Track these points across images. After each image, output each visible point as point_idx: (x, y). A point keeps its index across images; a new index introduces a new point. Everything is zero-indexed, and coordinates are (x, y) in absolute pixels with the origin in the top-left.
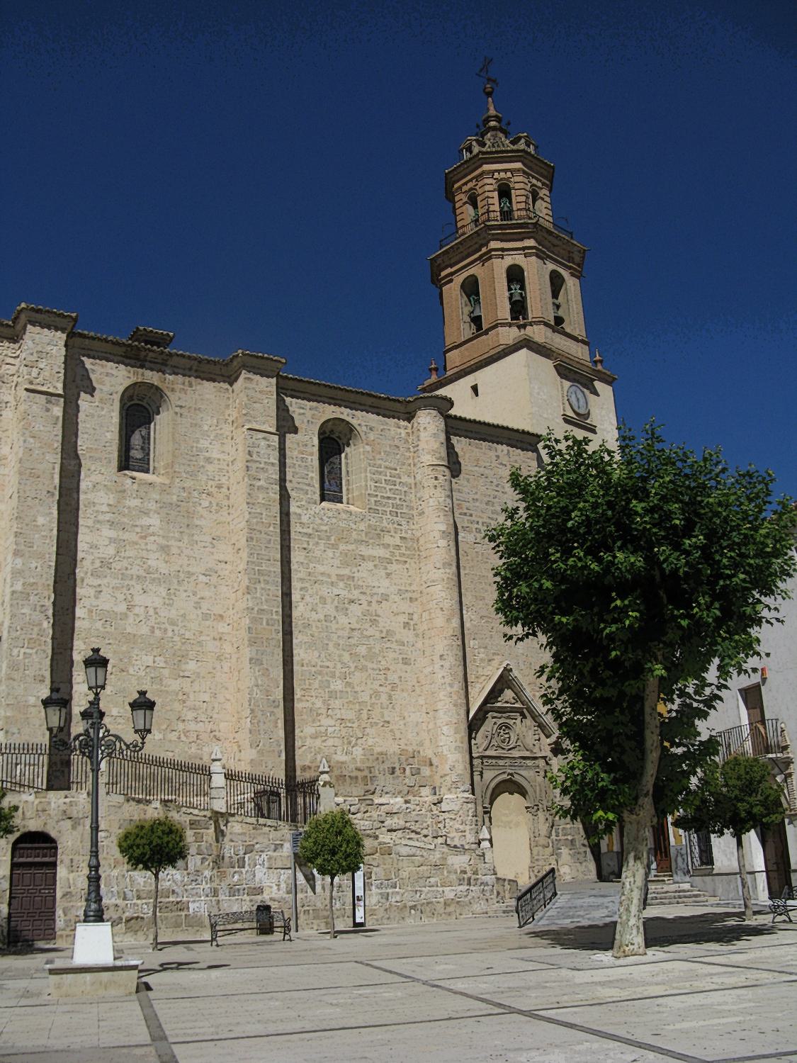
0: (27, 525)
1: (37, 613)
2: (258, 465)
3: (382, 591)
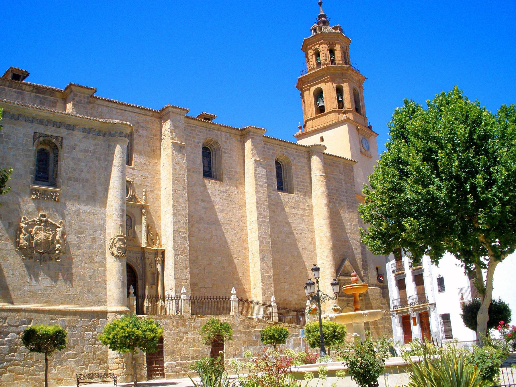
1: (183, 240)
3: (301, 228)
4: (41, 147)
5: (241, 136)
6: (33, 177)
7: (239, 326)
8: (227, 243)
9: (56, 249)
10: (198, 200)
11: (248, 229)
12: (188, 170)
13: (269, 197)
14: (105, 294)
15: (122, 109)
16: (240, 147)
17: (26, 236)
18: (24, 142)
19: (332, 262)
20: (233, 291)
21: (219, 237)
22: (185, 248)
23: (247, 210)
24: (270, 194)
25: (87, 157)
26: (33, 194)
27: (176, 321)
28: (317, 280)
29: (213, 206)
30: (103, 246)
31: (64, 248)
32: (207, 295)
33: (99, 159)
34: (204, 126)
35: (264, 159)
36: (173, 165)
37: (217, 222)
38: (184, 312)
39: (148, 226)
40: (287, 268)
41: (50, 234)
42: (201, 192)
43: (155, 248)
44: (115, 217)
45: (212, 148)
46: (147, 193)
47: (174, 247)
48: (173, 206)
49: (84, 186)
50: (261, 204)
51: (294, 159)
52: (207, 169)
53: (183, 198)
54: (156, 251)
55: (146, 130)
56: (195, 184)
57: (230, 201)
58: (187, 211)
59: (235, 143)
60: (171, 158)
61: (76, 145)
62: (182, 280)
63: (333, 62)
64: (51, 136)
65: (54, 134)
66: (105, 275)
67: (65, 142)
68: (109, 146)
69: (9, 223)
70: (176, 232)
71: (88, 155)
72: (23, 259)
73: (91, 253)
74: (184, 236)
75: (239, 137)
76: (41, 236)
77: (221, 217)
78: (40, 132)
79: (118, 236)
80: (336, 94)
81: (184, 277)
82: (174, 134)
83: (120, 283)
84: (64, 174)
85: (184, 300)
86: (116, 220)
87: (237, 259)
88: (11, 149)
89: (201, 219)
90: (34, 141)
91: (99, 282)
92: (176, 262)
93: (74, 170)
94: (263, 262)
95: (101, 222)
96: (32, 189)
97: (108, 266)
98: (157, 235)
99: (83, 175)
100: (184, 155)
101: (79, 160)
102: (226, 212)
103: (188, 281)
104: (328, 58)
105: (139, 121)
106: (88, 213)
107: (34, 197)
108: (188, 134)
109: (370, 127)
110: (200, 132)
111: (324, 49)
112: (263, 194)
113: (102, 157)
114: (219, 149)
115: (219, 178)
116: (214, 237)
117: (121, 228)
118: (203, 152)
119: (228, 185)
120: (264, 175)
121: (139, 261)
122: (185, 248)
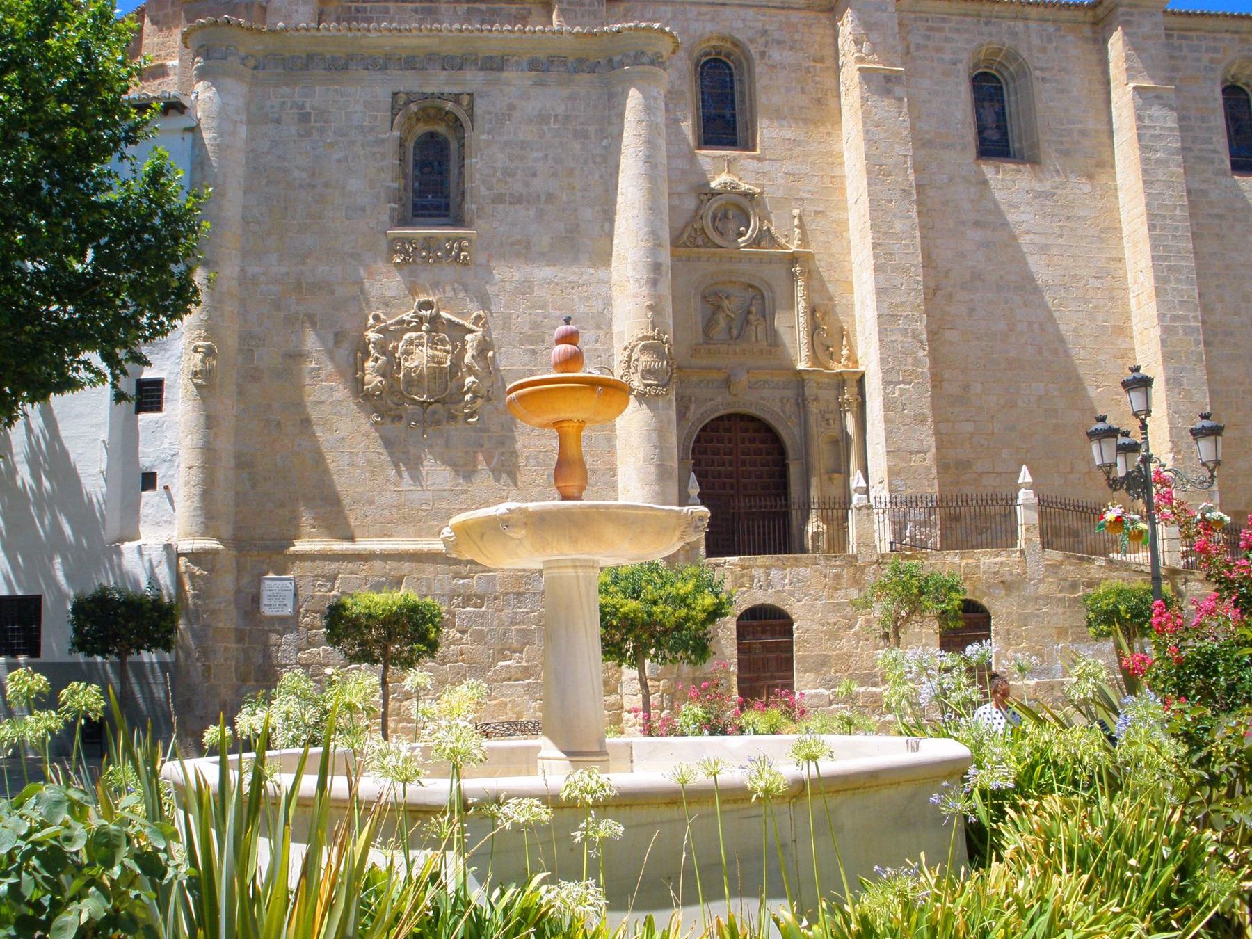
0: (885, 233)
1: (909, 340)
2: (1152, 132)
4: (422, 129)
5: (1095, 24)
6: (394, 209)
7: (1041, 581)
8: (1062, 341)
9: (466, 388)
10: (963, 223)
11: (1132, 295)
17: (379, 362)
18: (365, 124)
20: (1025, 476)
21: (1036, 326)
22: (917, 363)
23: (1125, 240)
25: (548, 136)
26: (396, 252)
27: (831, 572)
28: (1143, 422)
29: (1014, 238)
31: (489, 384)
33: (582, 135)
34: (970, 12)
35: (1170, 80)
36: (867, 132)
37: (1027, 285)
38: (858, 544)
39: (812, 311)
41: (445, 351)
43: (837, 368)
44: (632, 288)
45: (1006, 74)
46: (806, 219)
47: (883, 361)
48: (875, 246)
49: (541, 214)
50: (1164, 217)
52: (993, 135)
53: (906, 222)
54: (840, 378)
55: (791, 49)
56: (951, 180)
57: (1068, 218)
58: (920, 258)
59: (1075, 49)
60: (860, 113)
61: (512, 107)
62: (911, 453)
64: (441, 96)
65: (446, 90)
66: (612, 450)
67: (480, 106)
68: (611, 96)
69: (336, 334)
70: (886, 320)
71: (550, 129)
72: (376, 422)
74: (914, 330)
75: (1087, 31)
76: (420, 358)
77: (1036, 263)
78: (407, 89)
81: (915, 446)
82: (866, 47)
83: (653, 469)
84: (482, 188)
85: (859, 509)
86: (635, 296)
87: (1098, 387)
88: (332, 145)
89: (977, 276)
90: (394, 115)
92: (888, 405)
93: (509, 173)
94: (1177, 391)
95: (596, 306)
96: (395, 239)
98: (842, 333)
99: (538, 184)
100: (901, 100)
101: (524, 145)
102: (1054, 251)
103: (930, 455)
106: (557, 284)
107: (398, 261)
108: (921, 41)
110: (958, 31)
112: (1169, 185)
113: (592, 129)
114: (1023, 72)
115: (1029, 157)
117: (650, 314)
119: (1057, 171)
120: (1171, 129)
121: (791, 408)
122: (917, 363)
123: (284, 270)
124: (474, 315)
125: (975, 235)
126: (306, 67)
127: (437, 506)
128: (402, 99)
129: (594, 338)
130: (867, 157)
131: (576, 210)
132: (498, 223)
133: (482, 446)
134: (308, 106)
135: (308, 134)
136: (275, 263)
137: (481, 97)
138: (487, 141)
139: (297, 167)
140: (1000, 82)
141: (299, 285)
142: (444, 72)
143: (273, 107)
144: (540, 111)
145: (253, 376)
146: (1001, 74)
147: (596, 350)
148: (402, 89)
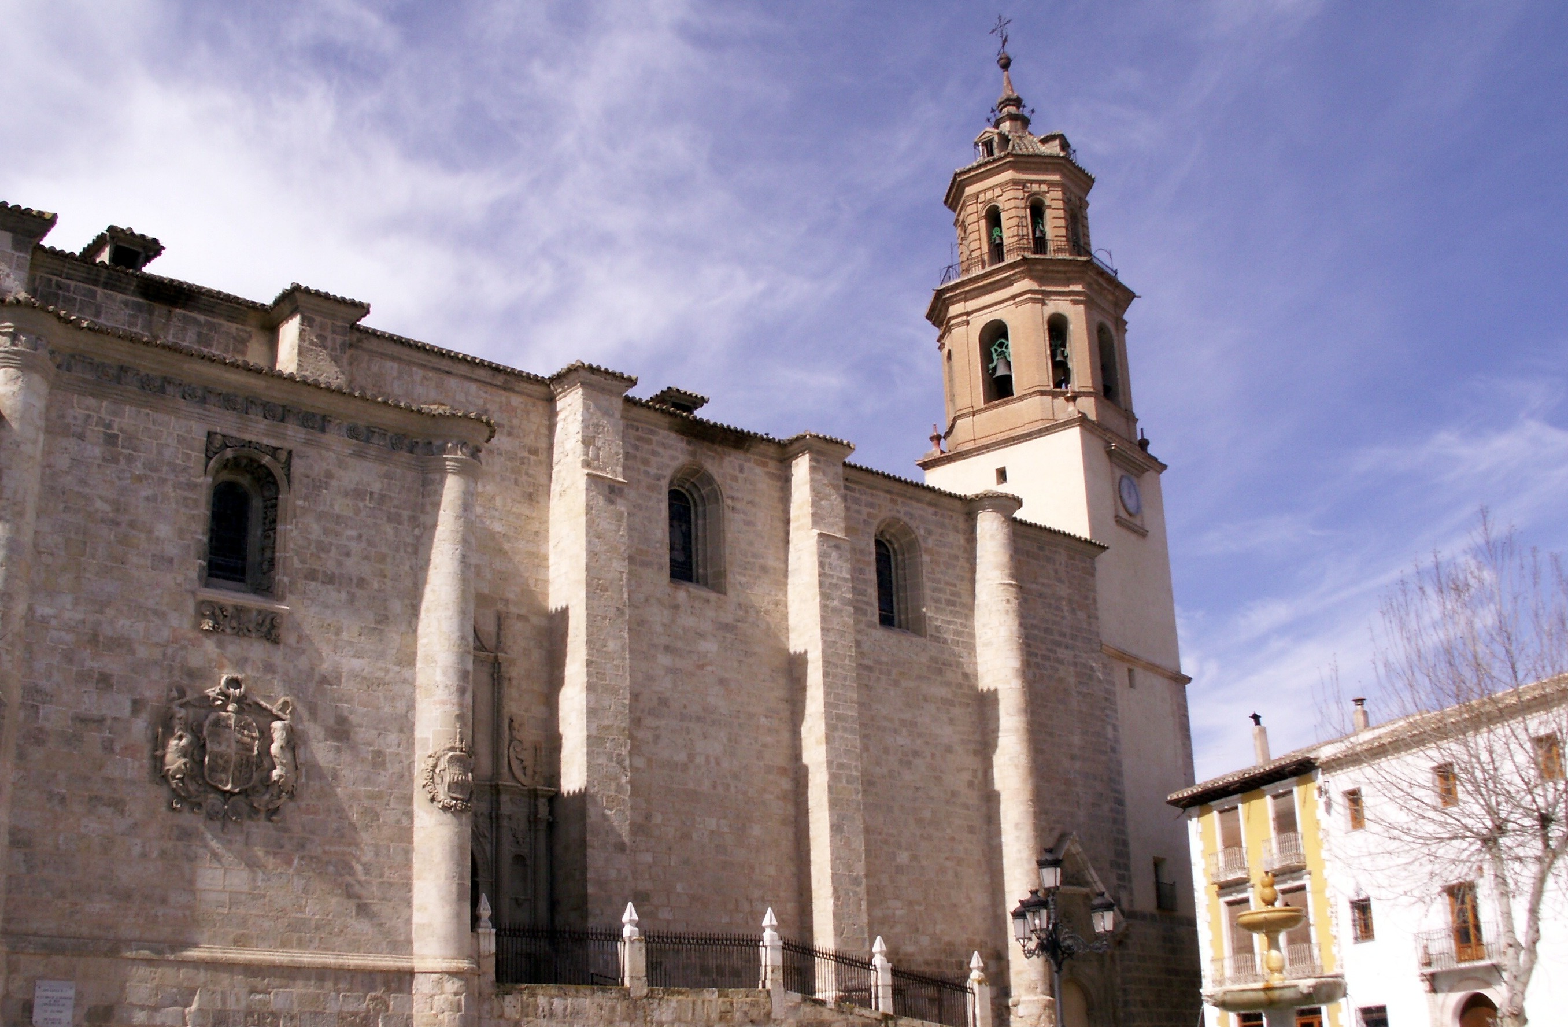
0: (598, 651)
1: (614, 764)
4: (226, 476)
6: (204, 567)
10: (655, 646)
12: (631, 559)
13: (858, 644)
14: (409, 921)
15: (439, 370)
16: (776, 494)
18: (179, 462)
19: (1032, 842)
21: (712, 760)
24: (859, 637)
25: (364, 514)
26: (204, 616)
30: (405, 776)
32: (680, 928)
33: (394, 519)
36: (589, 542)
38: (631, 978)
40: (903, 857)
42: (664, 625)
44: (441, 694)
45: (696, 496)
49: (352, 599)
50: (836, 666)
51: (929, 533)
52: (680, 558)
55: (510, 434)
56: (647, 600)
61: (329, 475)
63: (1040, 244)
64: (259, 447)
65: (265, 441)
66: (408, 864)
67: (298, 466)
68: (426, 482)
69: (135, 702)
70: (594, 742)
71: (366, 506)
73: (373, 797)
74: (619, 755)
78: (225, 431)
79: (452, 749)
80: (1048, 343)
84: (296, 560)
86: (443, 703)
88: (140, 479)
89: (663, 702)
90: (209, 458)
91: (391, 885)
93: (323, 547)
94: (839, 837)
95: (401, 706)
96: (203, 602)
97: (418, 837)
99: (352, 566)
101: (338, 519)
104: (1025, 233)
105: (488, 406)
106: (365, 678)
107: (206, 627)
109: (1144, 444)
110: (664, 446)
111: (1012, 203)
112: (842, 634)
113: (406, 514)
116: (700, 760)
118: (671, 505)
120: (845, 580)
122: (619, 789)
123: (79, 616)
124: (281, 701)
125: (664, 660)
126: (118, 380)
127: (233, 910)
128: (218, 442)
129: (396, 742)
130: (588, 568)
131: (385, 600)
132: (310, 602)
133: (282, 847)
134: (116, 426)
135: (115, 460)
136: (69, 606)
137: (300, 457)
138: (303, 508)
139: (101, 498)
140: (688, 503)
141: (94, 638)
142: (266, 421)
143: (75, 418)
144: (357, 484)
145: (38, 737)
146: (692, 496)
147: (398, 754)
148: (218, 430)
